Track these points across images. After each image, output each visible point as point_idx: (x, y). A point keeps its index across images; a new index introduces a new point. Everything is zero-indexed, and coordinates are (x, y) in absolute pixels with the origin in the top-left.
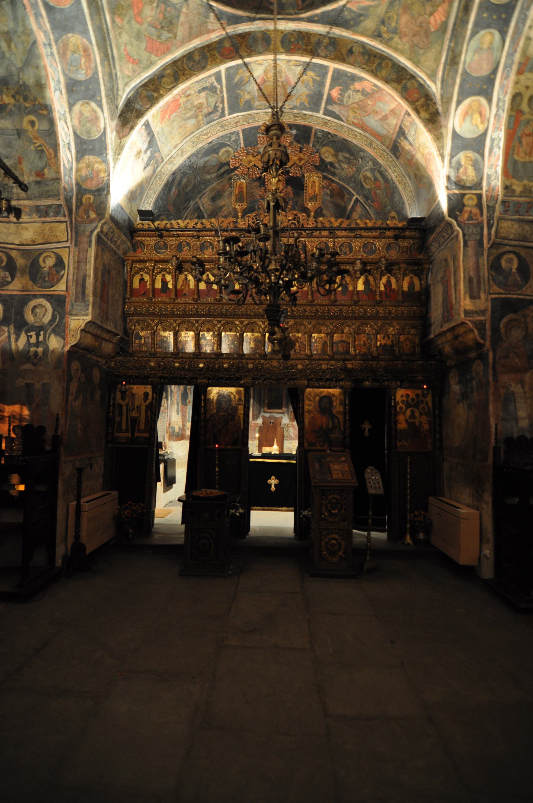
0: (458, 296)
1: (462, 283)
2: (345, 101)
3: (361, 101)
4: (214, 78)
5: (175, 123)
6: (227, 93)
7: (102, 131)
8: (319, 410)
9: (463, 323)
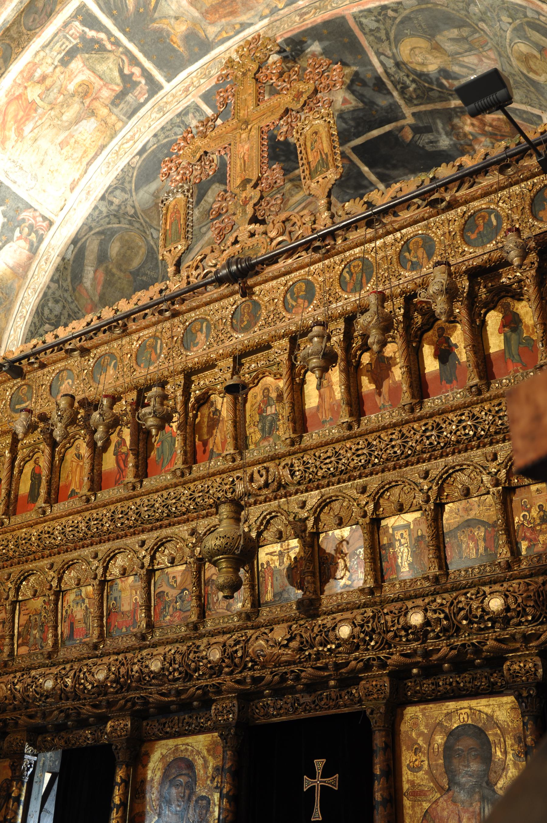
4: (77, 23)
5: (43, 143)
6: (131, 40)
8: (444, 782)
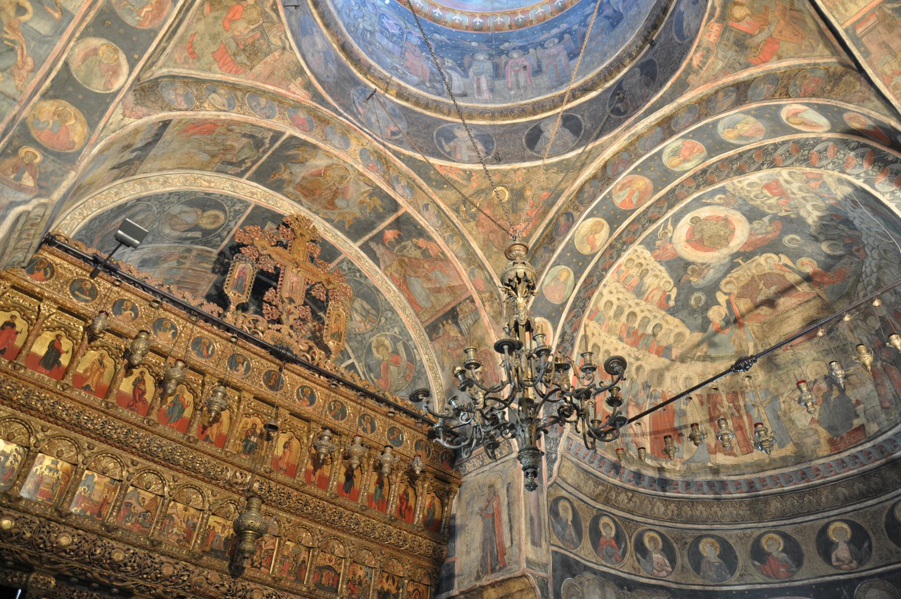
0: (516, 538)
1: (523, 521)
2: (397, 248)
3: (416, 259)
7: (113, 91)
9: (524, 576)
